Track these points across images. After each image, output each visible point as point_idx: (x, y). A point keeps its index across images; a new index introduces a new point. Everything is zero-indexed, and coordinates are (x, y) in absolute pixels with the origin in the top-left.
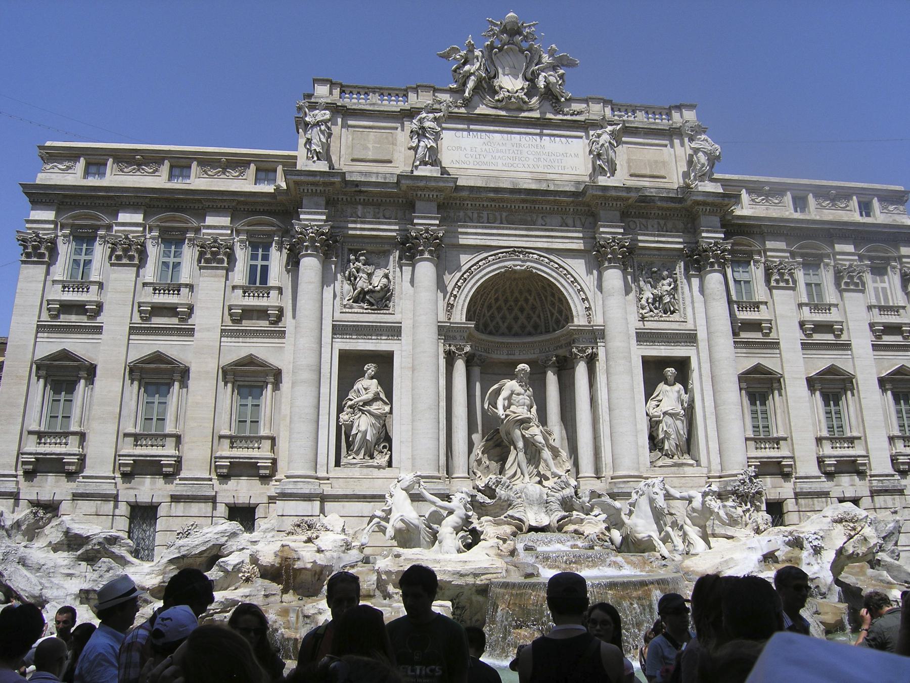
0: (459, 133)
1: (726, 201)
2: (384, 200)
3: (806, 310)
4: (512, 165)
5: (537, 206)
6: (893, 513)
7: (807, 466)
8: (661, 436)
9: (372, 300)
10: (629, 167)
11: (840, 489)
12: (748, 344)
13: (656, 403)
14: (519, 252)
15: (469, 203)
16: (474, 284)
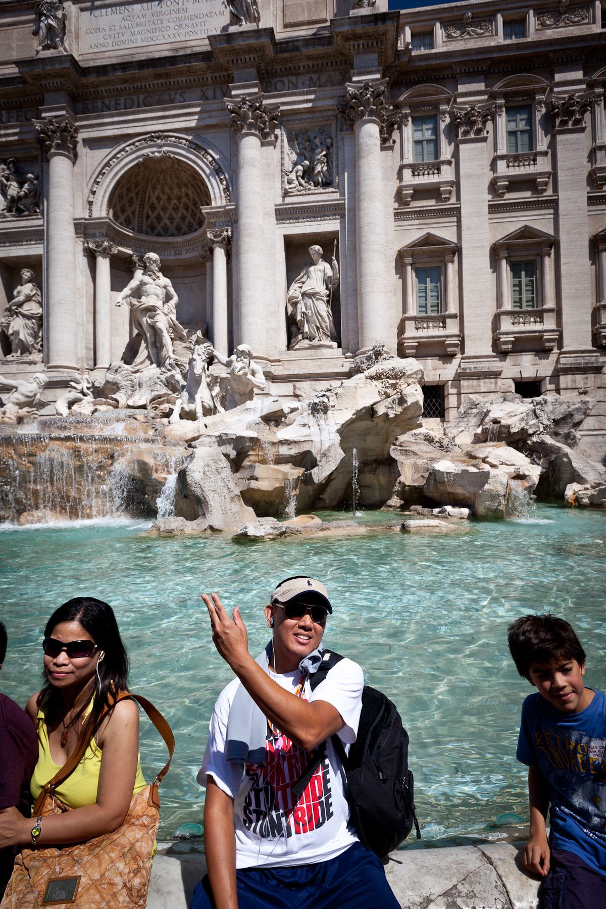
0: (97, 13)
1: (381, 27)
2: (22, 99)
3: (501, 165)
4: (152, 39)
5: (172, 80)
6: (581, 393)
7: (479, 343)
8: (299, 318)
9: (22, 207)
10: (284, 15)
11: (517, 369)
12: (421, 214)
13: (300, 285)
14: (158, 138)
15: (103, 89)
16: (113, 178)
